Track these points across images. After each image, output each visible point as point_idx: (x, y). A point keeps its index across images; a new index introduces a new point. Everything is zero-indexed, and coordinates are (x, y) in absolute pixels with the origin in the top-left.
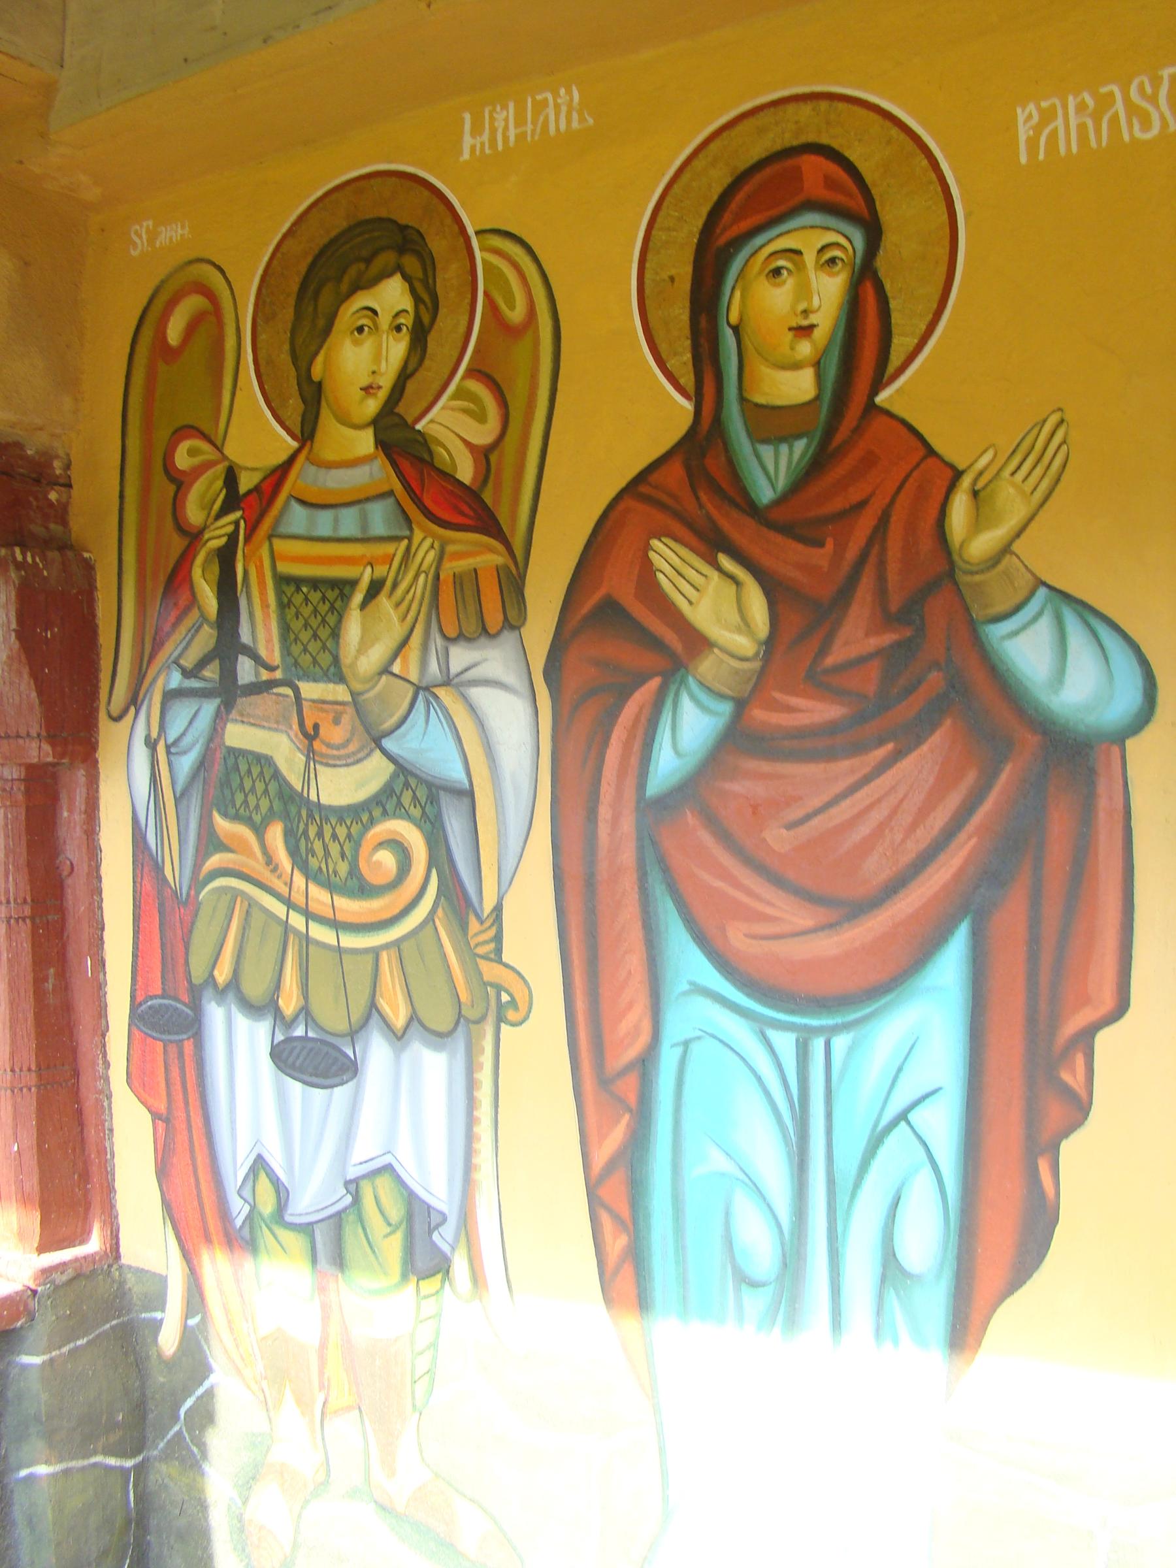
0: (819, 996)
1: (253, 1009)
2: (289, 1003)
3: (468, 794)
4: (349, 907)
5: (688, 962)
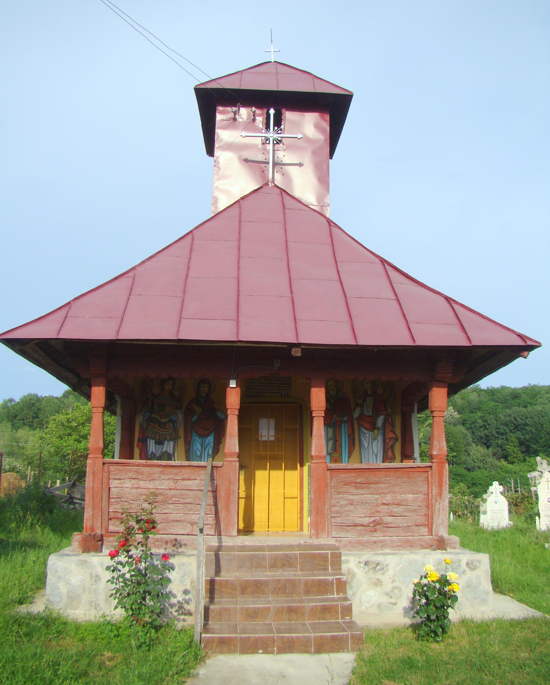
0: (203, 436)
1: (153, 439)
2: (157, 438)
3: (176, 422)
4: (164, 430)
5: (194, 434)
